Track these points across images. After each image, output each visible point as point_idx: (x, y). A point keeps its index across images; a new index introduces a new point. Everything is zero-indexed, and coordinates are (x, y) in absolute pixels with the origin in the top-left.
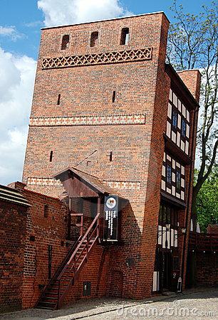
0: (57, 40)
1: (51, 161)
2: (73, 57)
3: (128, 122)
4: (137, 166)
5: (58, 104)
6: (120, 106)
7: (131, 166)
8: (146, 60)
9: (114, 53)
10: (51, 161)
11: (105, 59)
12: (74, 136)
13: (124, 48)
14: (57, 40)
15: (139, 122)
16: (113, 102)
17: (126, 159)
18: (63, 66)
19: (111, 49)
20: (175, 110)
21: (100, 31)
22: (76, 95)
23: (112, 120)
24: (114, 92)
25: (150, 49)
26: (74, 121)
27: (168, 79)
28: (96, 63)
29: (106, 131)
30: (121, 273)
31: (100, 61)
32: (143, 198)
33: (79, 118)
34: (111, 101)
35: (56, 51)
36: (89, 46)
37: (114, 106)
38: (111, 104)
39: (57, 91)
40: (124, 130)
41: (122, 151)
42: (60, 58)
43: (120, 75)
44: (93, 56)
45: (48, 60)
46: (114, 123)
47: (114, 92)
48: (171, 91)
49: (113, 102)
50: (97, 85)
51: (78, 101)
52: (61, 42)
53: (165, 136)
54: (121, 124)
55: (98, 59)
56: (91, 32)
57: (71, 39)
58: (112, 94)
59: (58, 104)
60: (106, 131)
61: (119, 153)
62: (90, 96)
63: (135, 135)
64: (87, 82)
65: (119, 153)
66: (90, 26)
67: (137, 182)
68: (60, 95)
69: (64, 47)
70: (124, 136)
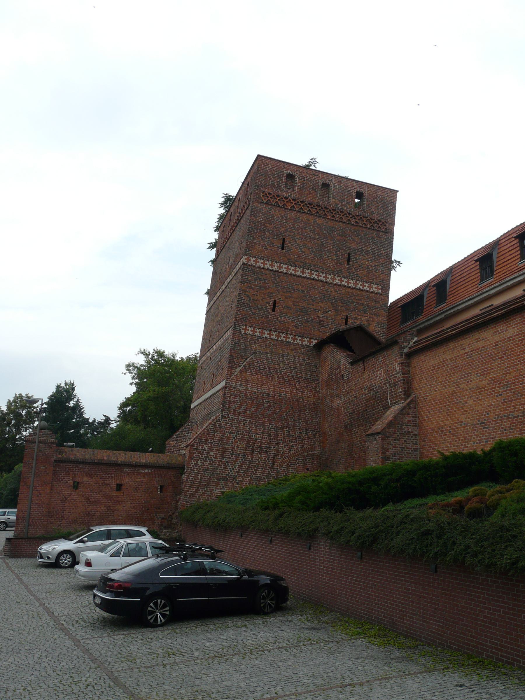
1: (274, 310)
5: (283, 248)
6: (356, 270)
8: (382, 231)
9: (349, 214)
10: (274, 310)
12: (303, 289)
16: (348, 264)
22: (304, 245)
23: (348, 282)
24: (349, 254)
25: (386, 222)
26: (303, 272)
28: (329, 217)
29: (340, 292)
31: (333, 216)
33: (309, 271)
34: (346, 262)
37: (349, 269)
43: (356, 238)
47: (349, 254)
49: (348, 264)
50: (330, 242)
54: (357, 289)
58: (346, 256)
59: (283, 248)
60: (340, 292)
64: (319, 234)
68: (284, 240)
70: (360, 302)
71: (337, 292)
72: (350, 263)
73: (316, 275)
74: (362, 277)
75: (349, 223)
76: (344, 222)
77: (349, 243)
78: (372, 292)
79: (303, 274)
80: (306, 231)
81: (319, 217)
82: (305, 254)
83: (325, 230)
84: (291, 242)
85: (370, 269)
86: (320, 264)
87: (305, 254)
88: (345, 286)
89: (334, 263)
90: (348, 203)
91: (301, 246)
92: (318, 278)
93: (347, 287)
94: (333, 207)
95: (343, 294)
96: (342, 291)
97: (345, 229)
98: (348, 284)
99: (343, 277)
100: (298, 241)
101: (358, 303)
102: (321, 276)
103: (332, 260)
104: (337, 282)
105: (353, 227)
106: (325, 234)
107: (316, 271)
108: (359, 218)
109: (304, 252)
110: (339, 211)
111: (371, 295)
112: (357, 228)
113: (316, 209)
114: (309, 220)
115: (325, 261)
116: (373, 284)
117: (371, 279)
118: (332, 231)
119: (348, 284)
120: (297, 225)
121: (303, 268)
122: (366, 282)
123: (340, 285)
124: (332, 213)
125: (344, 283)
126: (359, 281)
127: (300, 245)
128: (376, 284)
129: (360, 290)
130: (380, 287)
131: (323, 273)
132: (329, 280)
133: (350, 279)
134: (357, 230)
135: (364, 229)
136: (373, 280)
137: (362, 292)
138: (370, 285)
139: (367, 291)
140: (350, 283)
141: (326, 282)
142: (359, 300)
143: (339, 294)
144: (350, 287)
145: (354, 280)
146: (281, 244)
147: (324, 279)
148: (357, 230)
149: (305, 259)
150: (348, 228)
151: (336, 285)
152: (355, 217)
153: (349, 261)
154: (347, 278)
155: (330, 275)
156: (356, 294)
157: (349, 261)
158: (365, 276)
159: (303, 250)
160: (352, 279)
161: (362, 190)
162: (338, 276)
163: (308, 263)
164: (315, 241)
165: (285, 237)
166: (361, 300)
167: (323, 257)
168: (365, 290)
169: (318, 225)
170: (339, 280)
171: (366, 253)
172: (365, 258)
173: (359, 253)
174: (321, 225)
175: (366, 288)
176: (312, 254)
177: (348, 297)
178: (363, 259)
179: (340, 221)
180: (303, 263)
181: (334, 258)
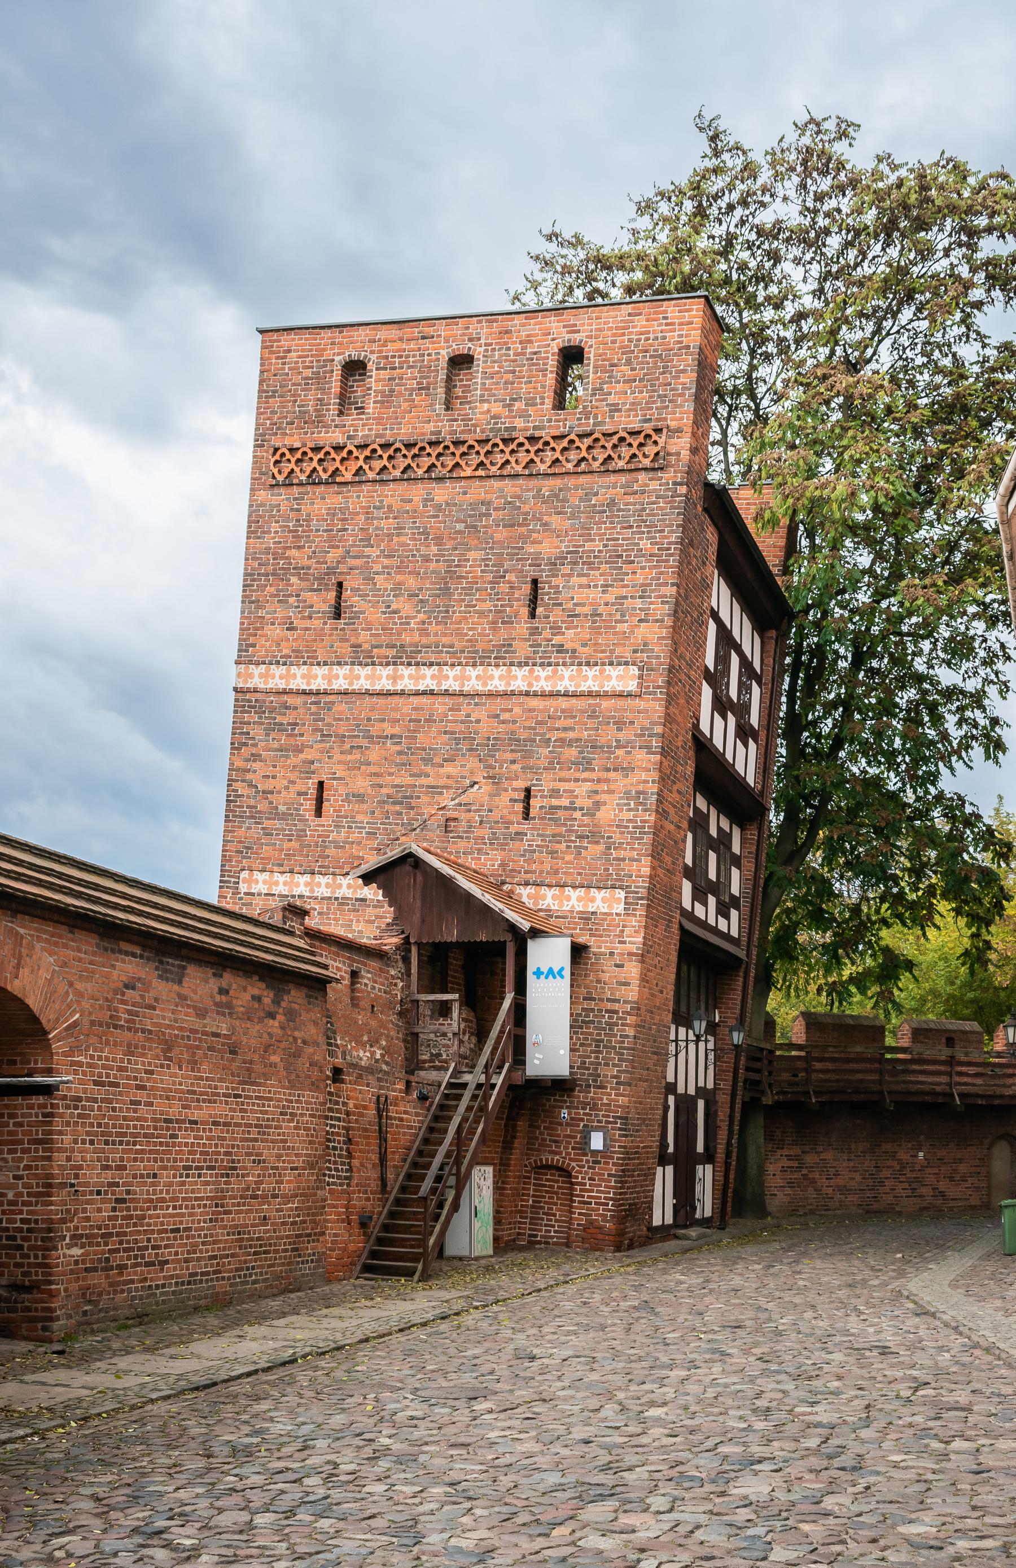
0: (320, 379)
2: (385, 446)
3: (584, 688)
4: (617, 838)
6: (556, 630)
7: (594, 836)
9: (532, 439)
11: (499, 459)
13: (569, 422)
14: (320, 379)
15: (619, 688)
16: (533, 615)
17: (577, 814)
18: (348, 476)
19: (519, 423)
20: (725, 637)
21: (478, 352)
22: (397, 589)
24: (535, 582)
27: (711, 535)
28: (469, 472)
30: (565, 1173)
32: (635, 941)
34: (525, 611)
35: (319, 421)
36: (439, 408)
37: (534, 631)
38: (522, 626)
39: (331, 571)
40: (568, 713)
41: (563, 786)
42: (338, 448)
43: (555, 521)
44: (457, 443)
45: (292, 450)
46: (535, 688)
47: (535, 582)
48: (716, 572)
49: (533, 615)
50: (472, 555)
51: (406, 607)
52: (335, 386)
53: (696, 726)
55: (474, 460)
56: (445, 354)
57: (375, 379)
58: (527, 589)
60: (505, 716)
61: (555, 793)
62: (446, 591)
63: (609, 735)
64: (439, 541)
65: (555, 793)
66: (442, 328)
67: (613, 887)
68: (340, 585)
69: (345, 402)
70: (571, 735)
71: (497, 716)
72: (540, 610)
73: (433, 677)
74: (574, 651)
75: (531, 475)
76: (516, 476)
77: (534, 542)
78: (606, 695)
79: (395, 683)
80: (402, 539)
81: (440, 479)
82: (400, 618)
83: (457, 521)
84: (358, 590)
85: (601, 615)
86: (445, 640)
87: (400, 618)
88: (521, 694)
89: (488, 623)
90: (531, 403)
91: (389, 595)
92: (439, 684)
93: (527, 694)
94: (483, 431)
95: (514, 722)
96: (511, 710)
97: (519, 497)
98: (530, 685)
99: (512, 664)
100: (379, 579)
101: (561, 740)
102: (447, 677)
103: (481, 613)
104: (497, 684)
105: (551, 482)
106: (459, 532)
107: (431, 664)
108: (565, 443)
109: (395, 612)
110: (498, 441)
111: (605, 704)
112: (558, 482)
113: (429, 455)
114: (410, 501)
115: (459, 623)
116: (611, 664)
117: (603, 652)
118: (481, 515)
119: (530, 685)
120: (377, 528)
121: (395, 664)
122: (588, 664)
123: (505, 694)
124: (478, 453)
125: (519, 684)
126: (564, 664)
127: (386, 590)
128: (619, 664)
129: (566, 695)
130: (634, 671)
131: (453, 665)
132: (473, 684)
133: (534, 665)
134: (560, 490)
135: (582, 479)
136: (612, 651)
137: (574, 700)
138: (602, 672)
139: (590, 694)
140: (538, 678)
141: (461, 694)
142: (565, 729)
143: (503, 722)
144: (535, 694)
145: (550, 664)
146: (333, 602)
147: (456, 687)
148: (560, 490)
149: (399, 634)
150: (528, 490)
151: (490, 695)
152: (553, 444)
153: (534, 601)
154: (527, 664)
155: (474, 665)
156: (556, 711)
157: (534, 601)
158: (584, 645)
159: (394, 606)
160: (542, 665)
161: (576, 339)
162: (497, 665)
163: (411, 645)
164: (427, 568)
165: (341, 578)
166: (572, 729)
167: (454, 612)
168: (582, 695)
169: (438, 508)
170: (501, 678)
171: (590, 563)
172: (584, 580)
173: (566, 569)
174: (447, 504)
175: (590, 682)
176: (419, 612)
177: (530, 728)
178: (581, 586)
179: (502, 476)
180: (394, 646)
181: (488, 605)
